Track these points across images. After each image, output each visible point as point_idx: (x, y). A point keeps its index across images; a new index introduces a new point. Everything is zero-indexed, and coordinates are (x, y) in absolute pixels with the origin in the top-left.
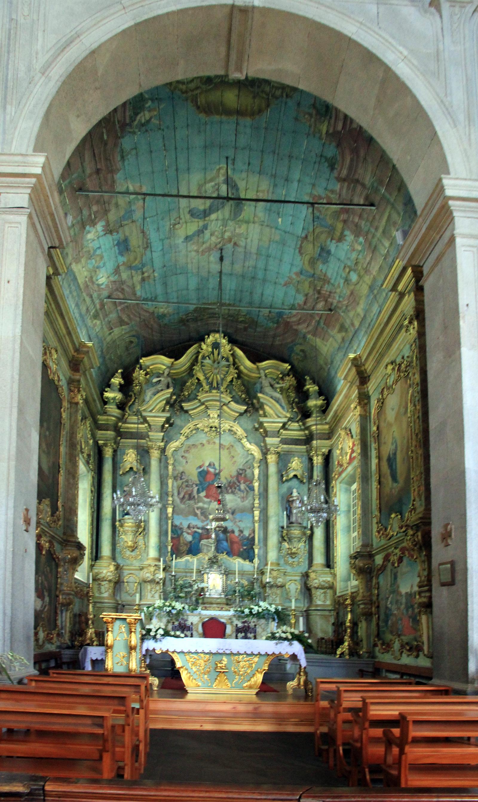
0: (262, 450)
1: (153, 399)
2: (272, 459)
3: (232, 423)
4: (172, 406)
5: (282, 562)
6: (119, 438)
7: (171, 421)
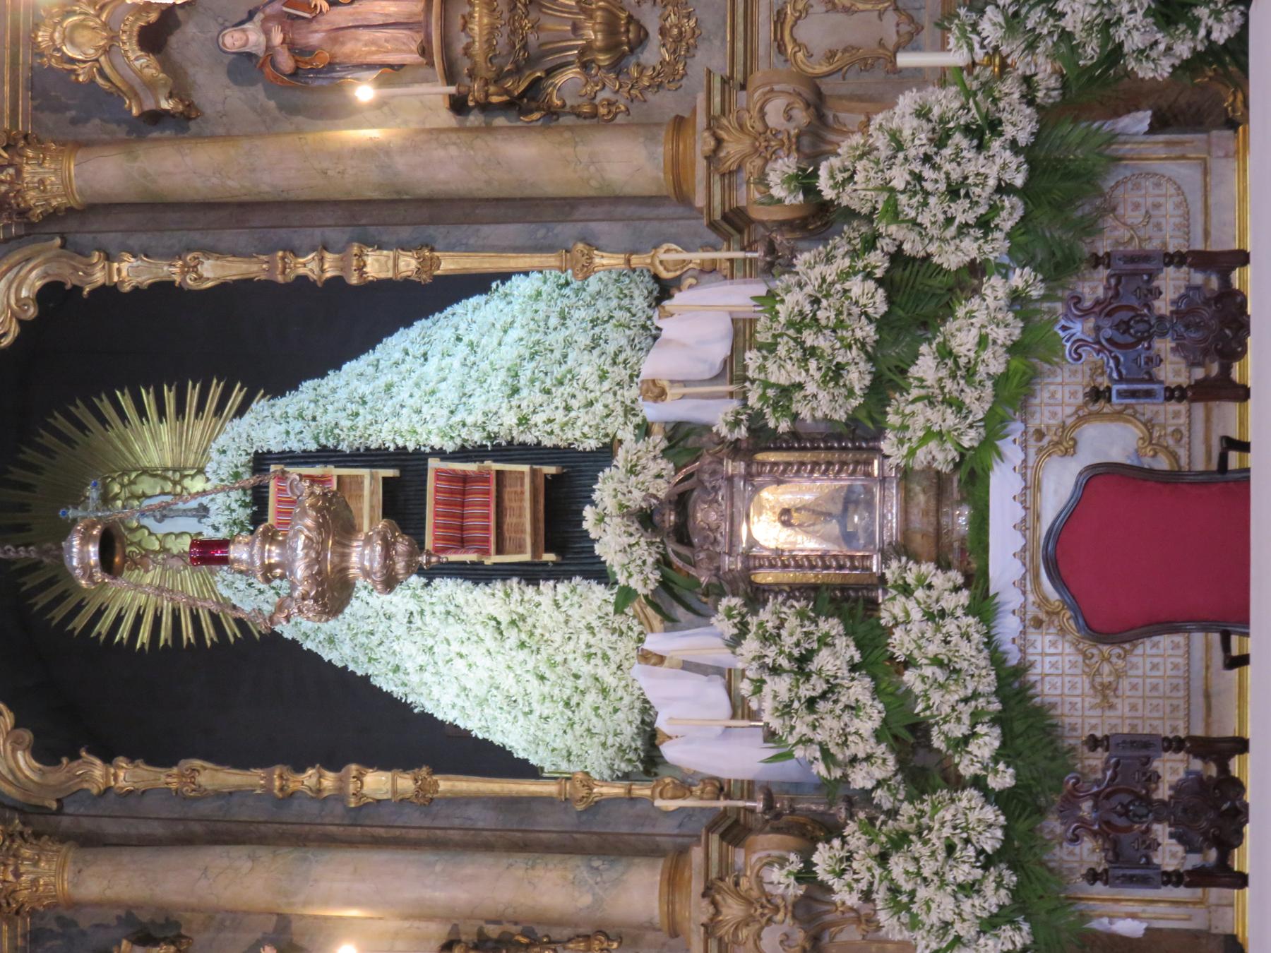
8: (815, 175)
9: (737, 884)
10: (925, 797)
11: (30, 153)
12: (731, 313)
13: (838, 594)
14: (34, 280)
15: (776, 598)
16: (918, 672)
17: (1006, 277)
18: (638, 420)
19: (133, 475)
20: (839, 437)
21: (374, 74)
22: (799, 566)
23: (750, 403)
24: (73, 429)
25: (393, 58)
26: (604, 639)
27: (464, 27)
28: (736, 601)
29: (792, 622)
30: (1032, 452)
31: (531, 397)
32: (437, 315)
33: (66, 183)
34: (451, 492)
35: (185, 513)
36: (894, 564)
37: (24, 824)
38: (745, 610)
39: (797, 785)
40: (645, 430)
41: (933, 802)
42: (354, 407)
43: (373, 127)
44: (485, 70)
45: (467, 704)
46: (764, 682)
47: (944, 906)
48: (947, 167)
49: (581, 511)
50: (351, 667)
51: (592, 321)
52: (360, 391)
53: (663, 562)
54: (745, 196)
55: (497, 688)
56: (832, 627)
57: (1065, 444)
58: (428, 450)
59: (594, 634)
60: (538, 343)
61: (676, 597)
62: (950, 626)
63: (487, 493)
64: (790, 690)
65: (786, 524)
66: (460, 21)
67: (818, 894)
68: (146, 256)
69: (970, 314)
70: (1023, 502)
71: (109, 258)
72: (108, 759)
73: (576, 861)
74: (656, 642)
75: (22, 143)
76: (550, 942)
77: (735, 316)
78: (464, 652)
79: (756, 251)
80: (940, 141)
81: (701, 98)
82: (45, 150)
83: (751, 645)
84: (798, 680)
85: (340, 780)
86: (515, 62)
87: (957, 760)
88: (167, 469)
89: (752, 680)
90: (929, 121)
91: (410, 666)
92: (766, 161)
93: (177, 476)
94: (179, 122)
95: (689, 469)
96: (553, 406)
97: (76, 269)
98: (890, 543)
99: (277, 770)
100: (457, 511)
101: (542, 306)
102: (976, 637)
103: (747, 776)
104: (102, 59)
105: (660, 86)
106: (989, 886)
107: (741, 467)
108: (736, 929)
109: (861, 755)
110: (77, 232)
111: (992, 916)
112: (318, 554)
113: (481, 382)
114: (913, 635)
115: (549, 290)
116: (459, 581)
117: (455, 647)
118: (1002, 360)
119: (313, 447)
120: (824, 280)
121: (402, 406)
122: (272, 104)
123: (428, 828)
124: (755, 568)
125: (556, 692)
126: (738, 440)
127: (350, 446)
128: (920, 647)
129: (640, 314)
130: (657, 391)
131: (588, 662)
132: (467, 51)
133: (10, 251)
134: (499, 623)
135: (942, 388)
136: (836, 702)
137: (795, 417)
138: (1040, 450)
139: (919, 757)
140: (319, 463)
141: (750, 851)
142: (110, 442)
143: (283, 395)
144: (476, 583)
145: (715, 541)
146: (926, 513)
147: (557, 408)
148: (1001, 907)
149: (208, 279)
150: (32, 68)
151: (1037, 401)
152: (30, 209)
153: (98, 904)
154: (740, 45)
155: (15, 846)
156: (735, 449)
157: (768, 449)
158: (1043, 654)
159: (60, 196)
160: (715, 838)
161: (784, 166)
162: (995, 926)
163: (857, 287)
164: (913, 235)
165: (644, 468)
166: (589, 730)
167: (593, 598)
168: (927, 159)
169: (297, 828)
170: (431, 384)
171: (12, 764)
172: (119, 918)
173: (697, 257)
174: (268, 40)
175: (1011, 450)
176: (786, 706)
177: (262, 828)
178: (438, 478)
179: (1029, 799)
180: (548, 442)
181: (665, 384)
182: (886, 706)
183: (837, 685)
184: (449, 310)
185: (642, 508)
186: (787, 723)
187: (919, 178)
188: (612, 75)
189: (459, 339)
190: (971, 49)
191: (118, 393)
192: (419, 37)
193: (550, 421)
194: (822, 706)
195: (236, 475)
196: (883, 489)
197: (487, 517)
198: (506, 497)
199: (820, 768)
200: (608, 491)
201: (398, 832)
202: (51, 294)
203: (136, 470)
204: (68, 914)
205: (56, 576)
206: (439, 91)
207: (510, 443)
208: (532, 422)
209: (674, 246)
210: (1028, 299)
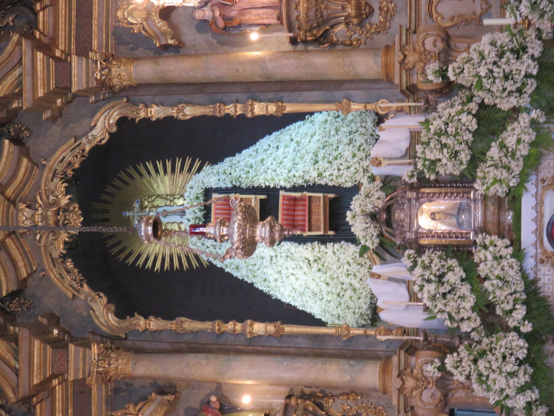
0: (107, 100)
2: (123, 73)
5: (382, 39)
7: (45, 321)
8: (447, 70)
9: (412, 372)
10: (494, 335)
11: (114, 63)
12: (409, 129)
13: (456, 249)
14: (115, 116)
15: (429, 250)
16: (490, 282)
17: (529, 113)
18: (369, 174)
19: (153, 198)
20: (456, 182)
21: (258, 28)
22: (439, 237)
23: (418, 167)
24: (128, 178)
25: (266, 21)
26: (354, 268)
27: (296, 8)
28: (412, 252)
29: (436, 260)
30: (540, 188)
31: (323, 164)
32: (282, 129)
33: (129, 75)
34: (290, 205)
36: (480, 236)
37: (112, 343)
38: (416, 255)
39: (437, 330)
40: (372, 179)
41: (497, 338)
42: (247, 169)
43: (257, 50)
44: (305, 26)
45: (295, 295)
46: (423, 286)
47: (501, 382)
48: (504, 66)
49: (346, 213)
50: (246, 279)
51: (349, 132)
52: (250, 162)
53: (381, 235)
54: (417, 79)
55: (308, 288)
56: (453, 263)
58: (279, 187)
59: (350, 266)
61: (386, 250)
62: (504, 262)
63: (305, 205)
64: (435, 289)
65: (433, 219)
66: (294, 6)
67: (447, 377)
68: (162, 105)
69: (513, 129)
70: (536, 210)
71: (147, 106)
72: (146, 317)
73: (343, 361)
74: (376, 269)
75: (111, 59)
76: (332, 396)
77: (411, 130)
78: (294, 273)
79: (421, 102)
80: (501, 55)
82: (121, 61)
83: (418, 270)
84: (438, 286)
85: (243, 326)
86: (318, 23)
87: (507, 319)
88: (167, 195)
89: (419, 285)
90: (496, 47)
91: (271, 279)
92: (425, 64)
93: (172, 198)
94: (176, 49)
95: (392, 195)
96: (333, 169)
97: (133, 111)
98: (478, 227)
99: (217, 322)
100: (292, 213)
101: (327, 126)
102: (515, 267)
103: (416, 326)
104: (144, 23)
105: (379, 32)
106: (521, 373)
107: (414, 194)
108: (412, 391)
109: (466, 317)
110: (133, 96)
111: (522, 386)
112: (243, 230)
113: (302, 158)
114: (488, 266)
116: (292, 243)
117: (291, 271)
118: (527, 149)
119: (230, 186)
120: (450, 115)
121: (268, 169)
122: (214, 41)
123: (280, 347)
124: (420, 238)
125: (334, 290)
126: (413, 183)
127: (246, 186)
128: (491, 272)
129: (370, 129)
130: (378, 162)
131: (348, 277)
132: (297, 18)
133: (105, 104)
134: (309, 261)
135: (501, 161)
136: (455, 295)
137: (437, 173)
138: (543, 187)
139: (491, 319)
140: (232, 192)
141: (418, 358)
142: (144, 184)
143: (217, 164)
144: (300, 244)
146: (494, 214)
147: (334, 169)
148: (526, 383)
150: (114, 27)
151: (542, 166)
152: (114, 86)
153: (143, 377)
154: (413, 14)
155: (108, 353)
156: (412, 187)
157: (425, 187)
158: (544, 275)
159: (127, 81)
160: (402, 353)
161: (433, 67)
162: (523, 391)
163: (464, 118)
164: (489, 96)
165: (372, 195)
166: (347, 306)
168: (495, 63)
169: (225, 347)
170: (281, 159)
171: (106, 318)
172: (150, 383)
173: (395, 105)
174: (214, 14)
175: (531, 187)
176: (433, 296)
177: (211, 346)
178: (284, 199)
179: (538, 337)
180: (330, 184)
181: (381, 159)
182: (476, 297)
183: (455, 288)
184: (287, 128)
185: (371, 212)
186: (434, 303)
187: (491, 71)
188: (359, 28)
189: (292, 140)
190: (516, 18)
191: (147, 163)
192: (277, 12)
193: (331, 175)
194: (449, 296)
195: (197, 198)
196: (475, 204)
197: (304, 215)
198: (313, 207)
199: (448, 323)
200: (357, 204)
201: (267, 349)
202: (122, 122)
204: (129, 381)
205: (121, 240)
206: (285, 35)
207: (314, 184)
208: (324, 175)
209: (385, 100)
210: (539, 123)
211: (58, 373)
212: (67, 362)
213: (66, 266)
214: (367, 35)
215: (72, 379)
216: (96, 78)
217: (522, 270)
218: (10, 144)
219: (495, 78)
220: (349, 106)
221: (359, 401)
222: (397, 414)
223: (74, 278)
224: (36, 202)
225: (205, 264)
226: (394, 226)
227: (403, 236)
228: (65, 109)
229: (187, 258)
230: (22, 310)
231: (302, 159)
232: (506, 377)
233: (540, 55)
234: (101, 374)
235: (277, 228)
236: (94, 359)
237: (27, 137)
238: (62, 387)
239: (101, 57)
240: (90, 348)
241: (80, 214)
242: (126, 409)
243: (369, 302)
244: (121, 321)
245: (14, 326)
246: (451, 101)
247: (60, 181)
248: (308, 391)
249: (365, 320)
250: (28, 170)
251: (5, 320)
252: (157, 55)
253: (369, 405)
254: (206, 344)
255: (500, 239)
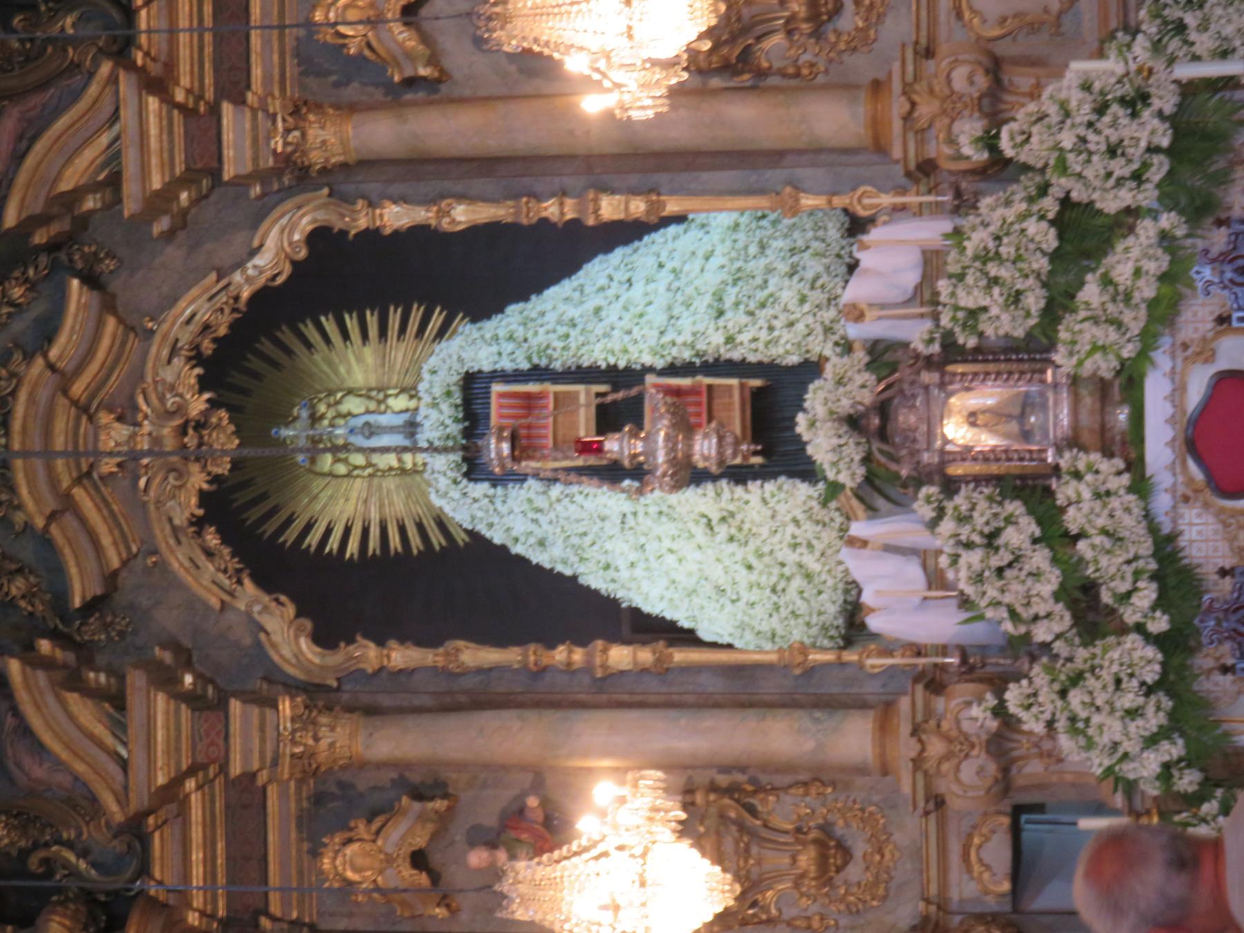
0: (287, 193)
1: (64, 755)
2: (327, 139)
3: (159, 350)
4: (86, 653)
5: (862, 66)
6: (265, 922)
7: (167, 657)
8: (998, 133)
9: (939, 726)
10: (1097, 642)
11: (311, 117)
12: (920, 246)
13: (1018, 482)
17: (1155, 219)
18: (836, 338)
19: (339, 395)
20: (1016, 350)
22: (986, 460)
26: (809, 529)
28: (933, 490)
29: (982, 505)
30: (1179, 360)
31: (734, 319)
32: (636, 244)
35: (392, 429)
36: (1067, 455)
38: (941, 497)
40: (847, 347)
45: (676, 596)
47: (1111, 729)
48: (1107, 131)
50: (559, 568)
51: (791, 250)
53: (867, 460)
54: (936, 148)
57: (1206, 353)
60: (739, 269)
61: (881, 487)
62: (1115, 503)
63: (699, 404)
64: (982, 561)
65: (973, 424)
69: (1127, 250)
70: (1173, 401)
71: (372, 205)
72: (381, 643)
74: (858, 529)
75: (304, 110)
76: (774, 789)
78: (675, 547)
79: (944, 195)
80: (1101, 109)
81: (896, 66)
82: (324, 114)
83: (947, 526)
85: (587, 654)
86: (731, 33)
87: (1122, 611)
88: (371, 389)
90: (1091, 93)
91: (622, 563)
92: (953, 120)
93: (381, 396)
95: (891, 379)
96: (757, 326)
97: (343, 216)
99: (532, 647)
101: (741, 236)
102: (1136, 511)
104: (370, 34)
105: (855, 49)
106: (1150, 710)
108: (939, 763)
109: (1042, 614)
115: (747, 221)
117: (667, 543)
119: (525, 366)
120: (1004, 221)
121: (613, 329)
124: (949, 462)
125: (763, 579)
126: (931, 355)
127: (563, 365)
129: (834, 244)
130: (857, 313)
134: (710, 520)
136: (1020, 569)
137: (981, 335)
138: (1186, 359)
139: (1089, 609)
142: (316, 365)
145: (914, 441)
146: (1092, 412)
148: (1161, 727)
149: (460, 223)
152: (310, 166)
154: (924, 13)
156: (930, 363)
157: (956, 362)
158: (1191, 524)
160: (920, 688)
163: (1033, 227)
165: (850, 380)
167: (791, 497)
168: (1090, 125)
172: (393, 781)
175: (1162, 357)
177: (520, 698)
180: (752, 358)
181: (864, 306)
182: (1063, 572)
184: (646, 239)
187: (1083, 140)
188: (812, 41)
189: (661, 266)
190: (1126, 63)
193: (755, 340)
194: (1008, 573)
195: (448, 394)
196: (1056, 393)
199: (1008, 626)
200: (818, 399)
201: (639, 698)
202: (318, 237)
203: (341, 390)
204: (346, 777)
205: (265, 493)
207: (717, 360)
209: (869, 188)
210: (1174, 238)
211: (205, 761)
212: (227, 737)
213: (204, 541)
214: (832, 55)
215: (238, 772)
216: (275, 151)
217: (1148, 516)
218: (81, 288)
219: (1090, 153)
220: (797, 200)
221: (830, 798)
222: (911, 809)
223: (223, 567)
224: (136, 408)
225: (461, 538)
226: (897, 440)
227: (916, 459)
228: (193, 211)
229: (420, 527)
230: (109, 638)
231: (688, 306)
232: (1122, 718)
233: (1175, 110)
234: (300, 758)
235: (729, 440)
236: (285, 728)
237: (111, 272)
238: (203, 795)
239: (284, 107)
240: (275, 706)
241: (233, 433)
242: (351, 829)
243: (842, 598)
244: (326, 652)
245: (97, 670)
246: (1005, 192)
247: (186, 364)
248: (723, 780)
249: (832, 638)
250: (118, 342)
251: (78, 658)
252: (389, 98)
253: (850, 804)
254: (511, 694)
255: (1105, 460)
